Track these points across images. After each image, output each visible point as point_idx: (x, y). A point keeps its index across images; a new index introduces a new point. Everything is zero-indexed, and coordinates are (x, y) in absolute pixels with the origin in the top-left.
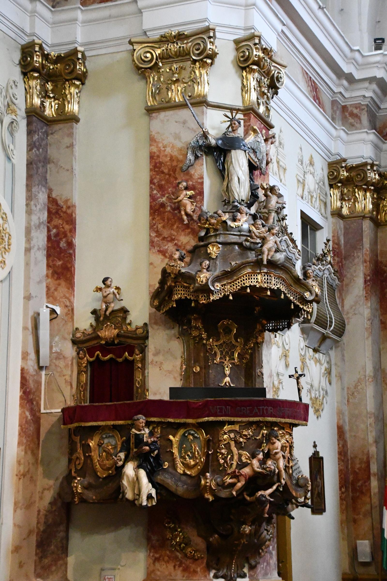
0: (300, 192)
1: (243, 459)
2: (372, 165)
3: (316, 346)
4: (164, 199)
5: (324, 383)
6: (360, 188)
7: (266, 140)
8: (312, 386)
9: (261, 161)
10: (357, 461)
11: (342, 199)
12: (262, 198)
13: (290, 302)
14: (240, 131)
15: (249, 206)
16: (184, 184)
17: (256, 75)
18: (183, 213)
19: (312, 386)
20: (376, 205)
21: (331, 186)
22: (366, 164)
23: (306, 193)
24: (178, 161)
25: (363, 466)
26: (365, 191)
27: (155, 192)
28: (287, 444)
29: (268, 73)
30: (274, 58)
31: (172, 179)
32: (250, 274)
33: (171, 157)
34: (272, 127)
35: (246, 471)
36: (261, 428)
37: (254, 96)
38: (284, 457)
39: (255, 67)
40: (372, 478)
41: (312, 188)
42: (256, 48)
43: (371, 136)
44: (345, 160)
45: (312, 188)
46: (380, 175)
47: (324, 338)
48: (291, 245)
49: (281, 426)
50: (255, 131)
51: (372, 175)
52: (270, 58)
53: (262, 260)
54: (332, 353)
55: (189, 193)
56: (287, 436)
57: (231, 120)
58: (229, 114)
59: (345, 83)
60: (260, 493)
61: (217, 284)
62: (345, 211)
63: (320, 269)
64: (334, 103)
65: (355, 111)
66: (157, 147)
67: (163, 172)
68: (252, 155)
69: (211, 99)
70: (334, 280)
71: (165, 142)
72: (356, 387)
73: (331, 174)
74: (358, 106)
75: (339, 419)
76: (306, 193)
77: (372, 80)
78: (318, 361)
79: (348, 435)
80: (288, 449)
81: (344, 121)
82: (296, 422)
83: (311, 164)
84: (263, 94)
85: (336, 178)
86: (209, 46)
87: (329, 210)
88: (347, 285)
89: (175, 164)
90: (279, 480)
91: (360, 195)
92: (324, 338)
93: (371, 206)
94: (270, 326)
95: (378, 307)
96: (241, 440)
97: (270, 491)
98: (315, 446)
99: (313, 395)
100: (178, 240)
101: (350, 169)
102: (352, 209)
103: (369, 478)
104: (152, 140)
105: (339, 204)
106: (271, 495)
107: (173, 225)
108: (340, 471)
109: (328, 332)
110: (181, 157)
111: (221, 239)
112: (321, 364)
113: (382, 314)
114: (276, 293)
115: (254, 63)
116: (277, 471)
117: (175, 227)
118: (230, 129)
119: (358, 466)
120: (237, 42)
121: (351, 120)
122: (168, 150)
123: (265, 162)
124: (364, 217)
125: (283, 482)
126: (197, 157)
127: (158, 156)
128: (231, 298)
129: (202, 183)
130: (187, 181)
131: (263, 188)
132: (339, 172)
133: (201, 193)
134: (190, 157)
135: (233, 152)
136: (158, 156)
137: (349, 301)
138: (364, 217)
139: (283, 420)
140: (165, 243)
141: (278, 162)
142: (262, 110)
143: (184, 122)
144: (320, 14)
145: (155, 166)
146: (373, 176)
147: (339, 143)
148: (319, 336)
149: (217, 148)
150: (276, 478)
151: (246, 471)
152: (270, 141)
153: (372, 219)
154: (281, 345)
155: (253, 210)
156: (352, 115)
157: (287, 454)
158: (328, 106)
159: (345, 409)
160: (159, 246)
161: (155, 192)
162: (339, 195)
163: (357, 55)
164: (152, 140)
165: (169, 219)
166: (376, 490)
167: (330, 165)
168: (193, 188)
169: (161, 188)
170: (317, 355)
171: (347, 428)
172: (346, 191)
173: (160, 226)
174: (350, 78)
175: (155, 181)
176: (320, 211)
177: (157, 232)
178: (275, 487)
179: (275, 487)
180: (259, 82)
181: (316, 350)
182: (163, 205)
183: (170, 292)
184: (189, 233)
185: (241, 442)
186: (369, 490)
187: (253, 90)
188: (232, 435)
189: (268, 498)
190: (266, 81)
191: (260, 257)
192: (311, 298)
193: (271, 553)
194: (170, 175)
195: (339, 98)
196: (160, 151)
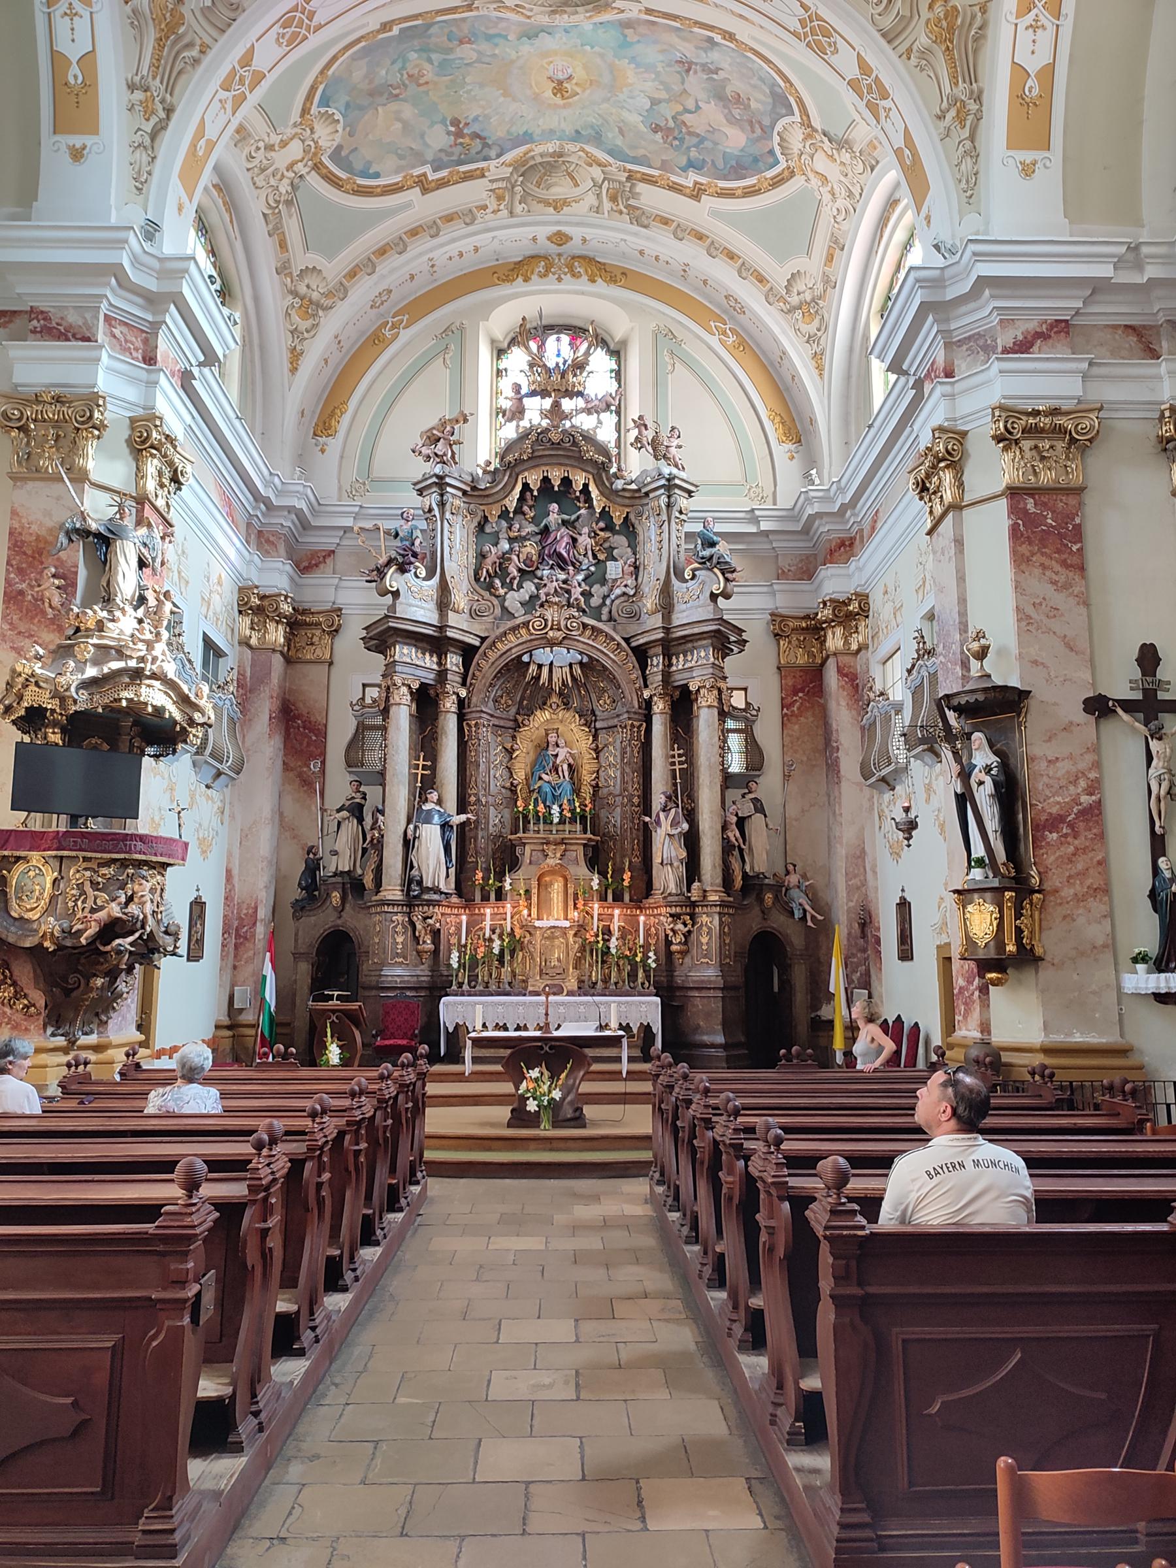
0: (204, 610)
1: (99, 902)
2: (286, 597)
3: (209, 782)
4: (24, 586)
5: (215, 822)
6: (272, 619)
7: (163, 538)
8: (200, 825)
9: (154, 559)
10: (245, 906)
11: (252, 629)
12: (152, 602)
13: (175, 723)
14: (129, 522)
15: (136, 608)
16: (53, 570)
17: (155, 461)
18: (47, 605)
19: (200, 825)
20: (288, 640)
21: (240, 612)
22: (280, 595)
23: (210, 613)
24: (46, 542)
25: (250, 911)
26: (277, 622)
27: (12, 576)
28: (159, 887)
29: (171, 464)
30: (178, 449)
31: (36, 563)
32: (128, 685)
33: (38, 536)
34: (171, 526)
35: (102, 915)
36: (127, 867)
37: (151, 485)
38: (152, 901)
39: (154, 452)
40: (258, 924)
41: (218, 610)
42: (157, 431)
43: (288, 568)
44: (257, 587)
45: (218, 610)
46: (294, 609)
47: (219, 774)
48: (188, 666)
49: (151, 865)
50: (149, 525)
51: (286, 607)
52: (175, 447)
53: (143, 669)
54: (227, 791)
55: (57, 582)
56: (159, 877)
57: (119, 506)
58: (118, 499)
59: (262, 506)
60: (118, 941)
61: (81, 691)
62: (254, 641)
63: (220, 698)
64: (249, 525)
65: (272, 539)
66: (20, 522)
67: (25, 553)
68: (143, 550)
69: (93, 477)
70: (235, 712)
71: (30, 519)
72: (250, 828)
73: (240, 599)
74: (274, 534)
75: (229, 862)
76: (210, 613)
77: (290, 509)
78: (208, 798)
79: (236, 880)
80: (159, 891)
81: (259, 547)
82: (171, 861)
83: (220, 583)
84: (162, 486)
85: (246, 603)
86: (96, 415)
87: (237, 637)
88: (250, 720)
89: (41, 545)
90: (143, 927)
91: (271, 626)
92: (219, 774)
93: (282, 640)
94: (150, 750)
95: (282, 746)
96: (100, 879)
97: (131, 939)
98: (198, 890)
99: (201, 836)
100: (39, 637)
101: (262, 598)
102: (262, 639)
103: (255, 924)
104: (14, 513)
105: (248, 632)
106: (131, 944)
107: (32, 618)
108: (225, 916)
109: (223, 767)
110: (50, 538)
111: (95, 641)
112: (214, 802)
113: (285, 755)
114: (159, 711)
115: (152, 447)
116: (141, 916)
117: (36, 620)
118: (118, 516)
119: (245, 911)
120: (133, 420)
121: (266, 547)
122: (34, 528)
123: (159, 560)
124: (274, 650)
125: (148, 929)
126: (71, 540)
127: (20, 534)
128: (100, 710)
129: (76, 573)
130: (56, 568)
131: (155, 591)
132: (249, 598)
133: (74, 585)
134: (63, 539)
135: (118, 543)
136: (20, 534)
137: (251, 737)
138: (274, 650)
139: (154, 859)
140: (21, 638)
141: (179, 573)
142: (160, 503)
143: (58, 498)
144: (237, 423)
145: (15, 545)
146: (286, 608)
147: (253, 568)
148: (215, 771)
149: (98, 535)
150: (139, 925)
151: (102, 915)
152: (167, 539)
153: (282, 653)
154: (166, 776)
155: (140, 613)
156: (268, 541)
157: (157, 898)
158: (243, 528)
159: (236, 851)
160: (13, 642)
161: (12, 576)
162: (249, 622)
163: (276, 480)
164: (14, 513)
165: (28, 611)
166: (262, 936)
167: (240, 589)
168: (63, 577)
169: (20, 571)
170: (209, 792)
171: (235, 872)
172: (256, 620)
173: (15, 617)
174: (267, 502)
175: (14, 562)
176: (226, 636)
177: (11, 624)
178: (137, 935)
179: (137, 935)
180: (160, 474)
181: (208, 787)
182: (21, 593)
183: (20, 698)
184: (54, 630)
185: (98, 883)
186: (254, 936)
187: (149, 477)
188: (88, 874)
189: (128, 947)
190: (167, 474)
191: (142, 665)
192: (201, 720)
193: (129, 1006)
194: (34, 558)
195: (255, 521)
196: (23, 528)
